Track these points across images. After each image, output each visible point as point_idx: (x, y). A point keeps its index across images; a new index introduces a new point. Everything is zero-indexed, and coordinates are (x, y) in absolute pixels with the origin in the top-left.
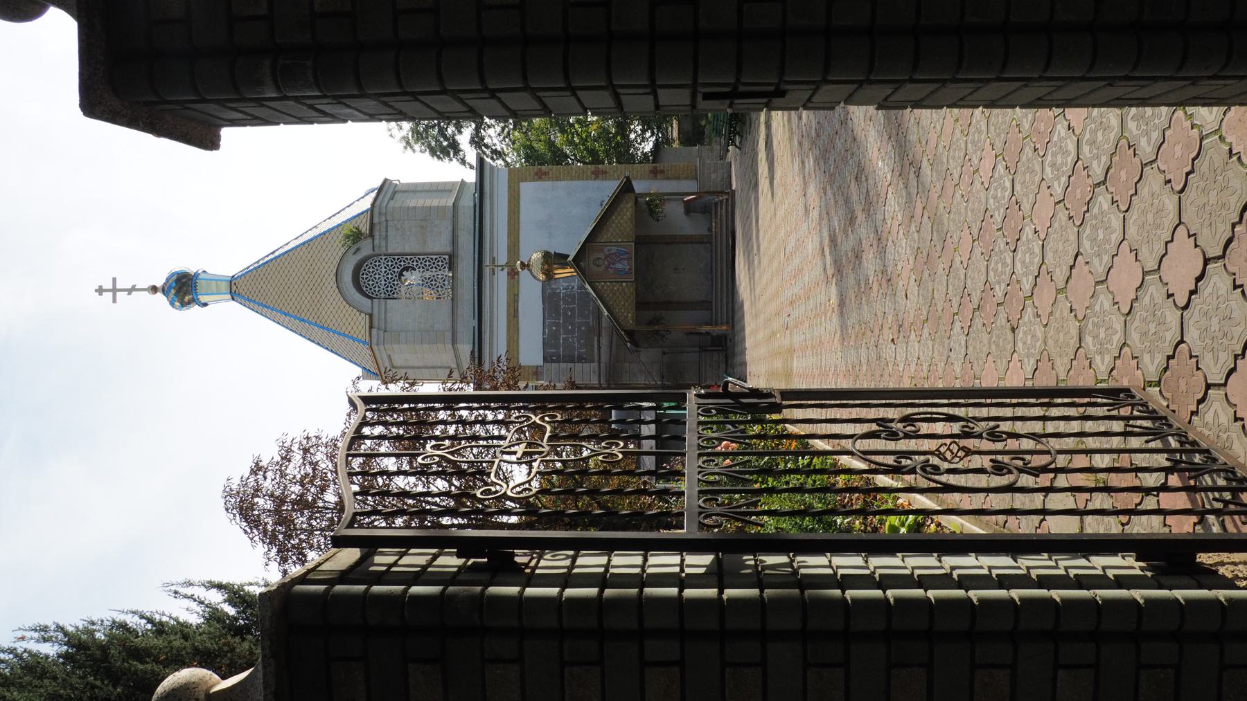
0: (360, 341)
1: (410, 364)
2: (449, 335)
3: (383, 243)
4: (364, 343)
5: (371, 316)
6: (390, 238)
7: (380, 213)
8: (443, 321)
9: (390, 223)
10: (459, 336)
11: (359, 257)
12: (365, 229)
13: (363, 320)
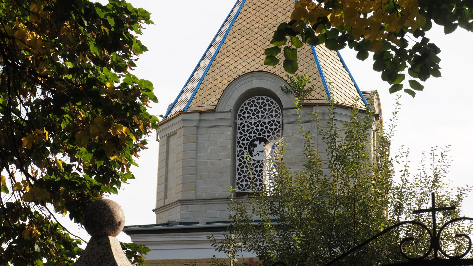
0: (190, 102)
1: (171, 155)
2: (191, 196)
3: (292, 119)
4: (188, 107)
5: (213, 111)
6: (298, 126)
7: (324, 113)
8: (207, 189)
9: (314, 124)
10: (189, 207)
11: (279, 94)
12: (316, 97)
13: (212, 102)
